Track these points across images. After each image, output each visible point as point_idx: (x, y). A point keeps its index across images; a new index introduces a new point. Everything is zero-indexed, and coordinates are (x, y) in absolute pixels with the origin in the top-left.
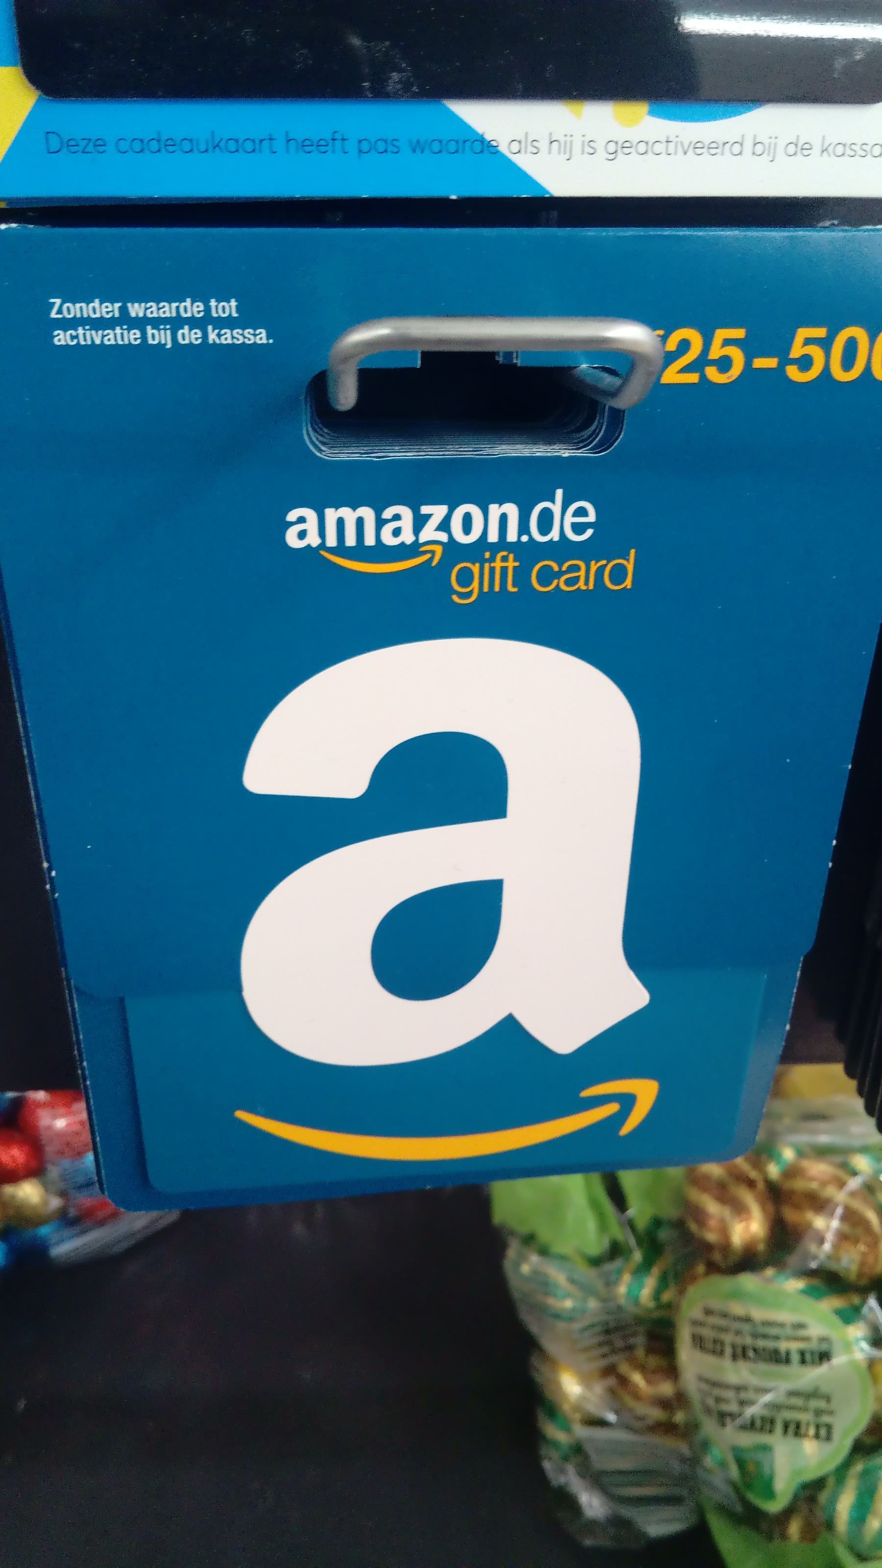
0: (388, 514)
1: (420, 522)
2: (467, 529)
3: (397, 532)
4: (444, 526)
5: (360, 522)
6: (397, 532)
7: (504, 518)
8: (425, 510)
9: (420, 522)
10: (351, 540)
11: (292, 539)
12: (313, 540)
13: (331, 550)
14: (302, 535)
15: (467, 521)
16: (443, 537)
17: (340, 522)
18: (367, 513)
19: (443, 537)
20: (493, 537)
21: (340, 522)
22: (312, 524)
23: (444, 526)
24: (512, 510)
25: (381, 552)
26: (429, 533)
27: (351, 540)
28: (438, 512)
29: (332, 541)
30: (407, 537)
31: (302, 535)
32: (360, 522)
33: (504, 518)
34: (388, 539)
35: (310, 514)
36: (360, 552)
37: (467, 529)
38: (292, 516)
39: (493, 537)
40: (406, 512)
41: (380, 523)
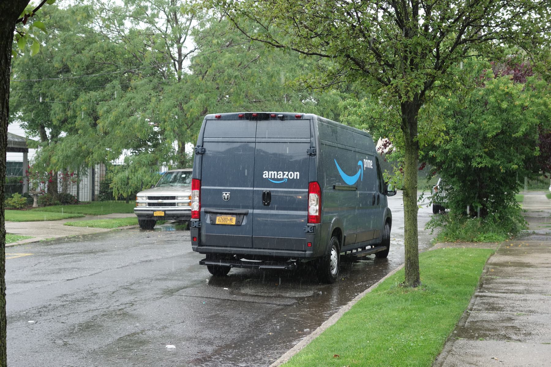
0: (279, 173)
1: (284, 174)
2: (291, 176)
3: (280, 176)
4: (288, 175)
5: (274, 174)
6: (280, 176)
7: (297, 174)
8: (285, 172)
9: (284, 174)
10: (273, 177)
11: (264, 177)
12: (267, 177)
13: (270, 179)
14: (266, 176)
15: (291, 174)
16: (287, 177)
17: (271, 174)
18: (276, 172)
19: (287, 177)
20: (295, 178)
21: (271, 174)
22: (267, 174)
23: (288, 175)
24: (298, 173)
25: (278, 179)
26: (285, 176)
27: (273, 177)
28: (286, 173)
29: (270, 177)
30: (282, 177)
31: (266, 176)
32: (274, 174)
33: (297, 174)
34: (279, 177)
35: (267, 172)
36: (274, 179)
37: (291, 176)
38: (264, 172)
39: (295, 178)
40: (281, 173)
41: (278, 174)
